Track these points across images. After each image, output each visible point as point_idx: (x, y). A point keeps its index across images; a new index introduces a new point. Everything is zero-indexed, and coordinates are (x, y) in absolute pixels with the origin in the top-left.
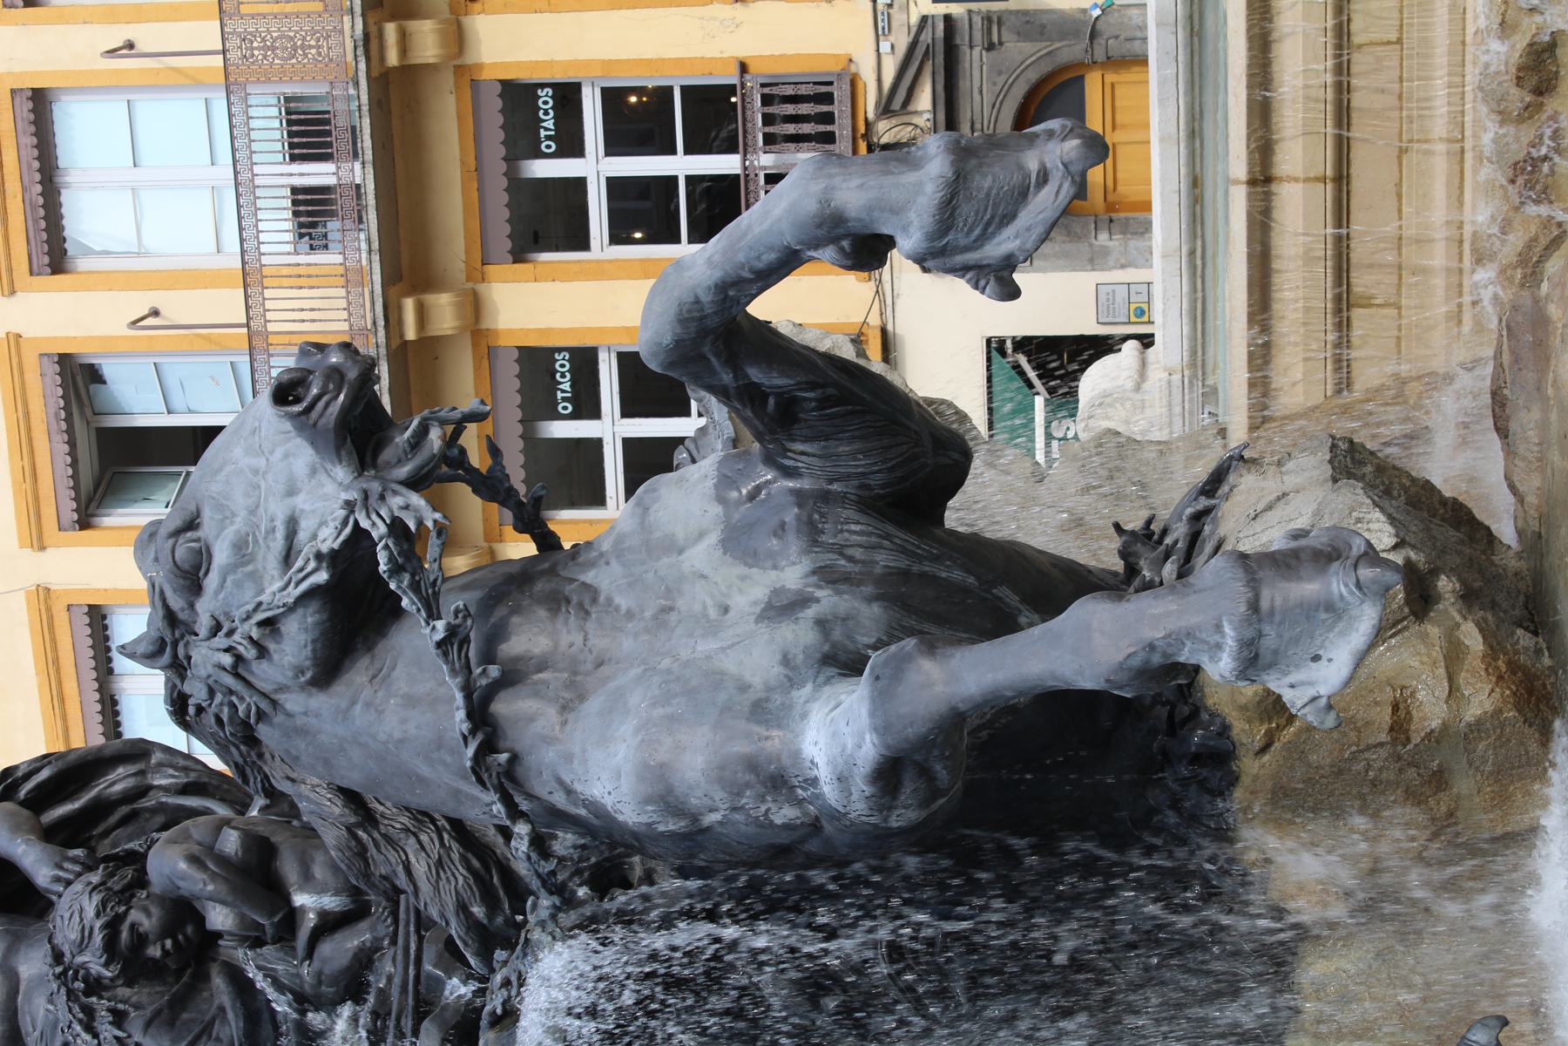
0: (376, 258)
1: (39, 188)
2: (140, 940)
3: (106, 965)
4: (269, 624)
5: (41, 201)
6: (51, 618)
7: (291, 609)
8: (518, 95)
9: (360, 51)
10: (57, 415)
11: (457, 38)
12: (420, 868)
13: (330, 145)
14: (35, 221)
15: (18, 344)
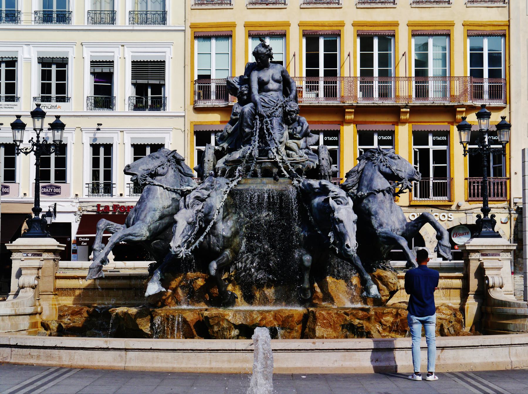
0: (309, 104)
2: (291, 115)
3: (288, 110)
4: (389, 167)
7: (391, 170)
8: (337, 133)
9: (350, 104)
10: (273, 32)
11: (349, 122)
12: (353, 179)
13: (331, 97)
14: (314, 32)
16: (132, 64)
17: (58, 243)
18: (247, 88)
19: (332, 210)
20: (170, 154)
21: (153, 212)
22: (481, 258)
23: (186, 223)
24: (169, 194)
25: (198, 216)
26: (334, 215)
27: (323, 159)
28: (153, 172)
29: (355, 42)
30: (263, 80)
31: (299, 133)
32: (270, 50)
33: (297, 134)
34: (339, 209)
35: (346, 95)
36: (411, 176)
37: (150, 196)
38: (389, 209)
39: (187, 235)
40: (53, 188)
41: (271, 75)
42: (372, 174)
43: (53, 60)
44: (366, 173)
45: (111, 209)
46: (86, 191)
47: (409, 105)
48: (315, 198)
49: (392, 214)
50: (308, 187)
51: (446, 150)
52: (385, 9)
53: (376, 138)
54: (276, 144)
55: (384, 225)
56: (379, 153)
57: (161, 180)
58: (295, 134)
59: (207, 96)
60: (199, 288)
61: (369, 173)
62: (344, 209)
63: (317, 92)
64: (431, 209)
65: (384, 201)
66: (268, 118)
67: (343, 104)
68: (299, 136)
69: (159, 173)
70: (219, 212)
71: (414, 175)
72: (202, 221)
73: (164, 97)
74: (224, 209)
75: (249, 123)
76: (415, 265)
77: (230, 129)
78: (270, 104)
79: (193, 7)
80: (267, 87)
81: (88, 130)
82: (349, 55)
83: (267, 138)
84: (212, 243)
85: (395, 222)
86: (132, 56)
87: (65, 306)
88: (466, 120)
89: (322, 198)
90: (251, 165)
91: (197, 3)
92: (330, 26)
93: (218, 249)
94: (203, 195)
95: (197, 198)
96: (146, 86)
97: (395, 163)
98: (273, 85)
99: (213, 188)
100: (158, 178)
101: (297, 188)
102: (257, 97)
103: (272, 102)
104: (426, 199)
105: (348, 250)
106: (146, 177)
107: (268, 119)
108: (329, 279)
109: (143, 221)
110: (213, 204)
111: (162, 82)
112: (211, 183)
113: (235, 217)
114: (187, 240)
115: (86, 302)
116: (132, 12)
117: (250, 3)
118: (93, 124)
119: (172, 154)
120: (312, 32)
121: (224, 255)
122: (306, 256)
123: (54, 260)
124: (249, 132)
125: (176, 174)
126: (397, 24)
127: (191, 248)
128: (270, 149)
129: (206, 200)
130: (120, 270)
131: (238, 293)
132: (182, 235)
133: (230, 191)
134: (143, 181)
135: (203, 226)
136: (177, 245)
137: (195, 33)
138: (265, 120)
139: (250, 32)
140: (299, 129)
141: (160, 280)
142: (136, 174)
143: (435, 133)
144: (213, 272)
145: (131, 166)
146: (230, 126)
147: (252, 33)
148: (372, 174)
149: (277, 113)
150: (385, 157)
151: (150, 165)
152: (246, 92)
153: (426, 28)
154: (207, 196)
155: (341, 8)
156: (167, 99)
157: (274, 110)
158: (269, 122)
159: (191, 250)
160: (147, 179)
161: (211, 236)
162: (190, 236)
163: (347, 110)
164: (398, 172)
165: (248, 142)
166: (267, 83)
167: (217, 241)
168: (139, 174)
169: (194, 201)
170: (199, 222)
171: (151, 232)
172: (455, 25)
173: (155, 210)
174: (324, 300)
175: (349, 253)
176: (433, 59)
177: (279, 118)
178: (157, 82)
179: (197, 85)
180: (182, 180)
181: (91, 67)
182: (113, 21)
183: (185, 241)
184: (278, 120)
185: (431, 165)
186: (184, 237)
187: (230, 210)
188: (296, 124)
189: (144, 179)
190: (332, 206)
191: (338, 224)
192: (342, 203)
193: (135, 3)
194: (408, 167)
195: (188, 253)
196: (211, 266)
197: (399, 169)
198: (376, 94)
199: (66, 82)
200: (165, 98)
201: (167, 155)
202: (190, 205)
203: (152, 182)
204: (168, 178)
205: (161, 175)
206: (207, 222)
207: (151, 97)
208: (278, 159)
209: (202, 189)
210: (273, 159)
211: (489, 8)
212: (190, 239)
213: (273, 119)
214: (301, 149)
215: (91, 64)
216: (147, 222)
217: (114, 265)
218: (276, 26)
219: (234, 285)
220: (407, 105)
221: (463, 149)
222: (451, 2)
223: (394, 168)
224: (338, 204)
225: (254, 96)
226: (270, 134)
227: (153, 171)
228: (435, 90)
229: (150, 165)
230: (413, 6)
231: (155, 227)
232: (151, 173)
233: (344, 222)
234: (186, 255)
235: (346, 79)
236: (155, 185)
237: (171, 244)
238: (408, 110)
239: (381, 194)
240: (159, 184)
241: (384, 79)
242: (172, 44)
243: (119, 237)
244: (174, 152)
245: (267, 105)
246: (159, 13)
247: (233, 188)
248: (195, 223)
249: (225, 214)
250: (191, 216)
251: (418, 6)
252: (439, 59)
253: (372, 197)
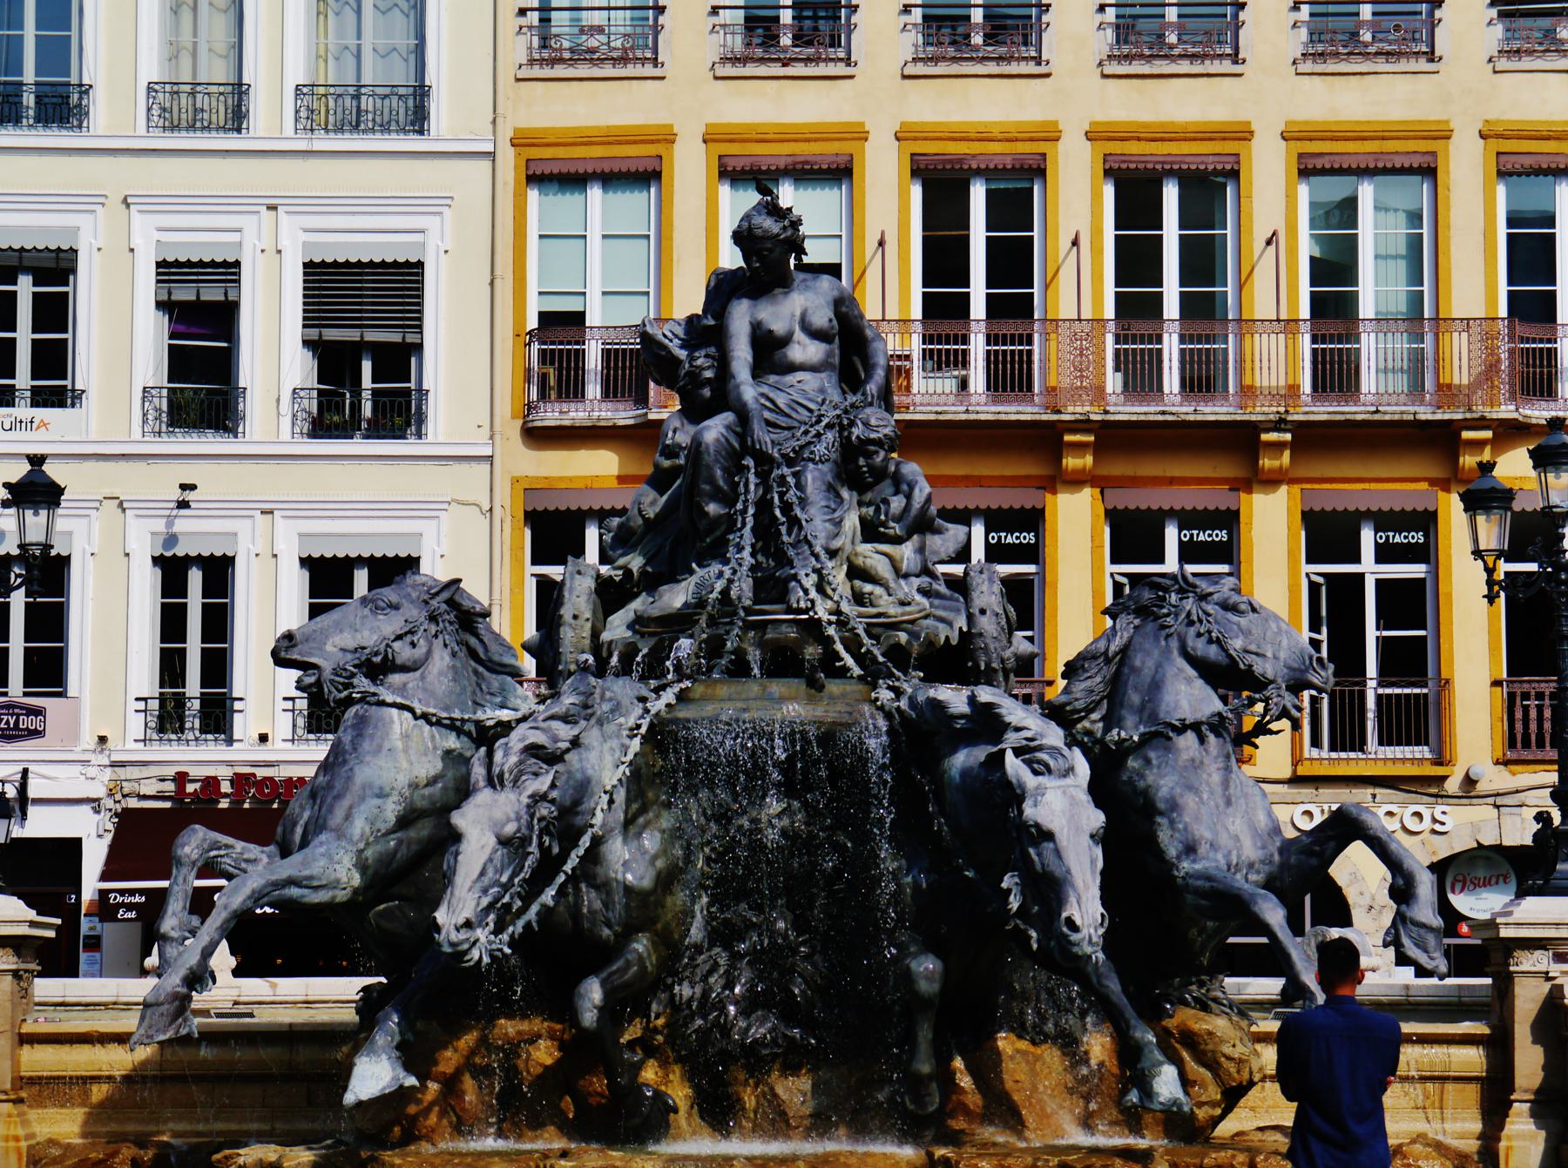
0: (932, 417)
1: (974, 166)
2: (869, 456)
3: (858, 437)
5: (966, 167)
6: (652, 142)
7: (1226, 651)
8: (1034, 519)
10: (807, 162)
11: (1076, 481)
12: (1088, 683)
13: (1013, 390)
14: (950, 161)
15: (861, 139)
16: (305, 274)
17: (31, 914)
18: (713, 358)
19: (1014, 795)
20: (437, 594)
21: (377, 801)
22: (1555, 969)
23: (492, 841)
24: (433, 737)
25: (538, 815)
26: (1021, 812)
27: (983, 612)
28: (377, 659)
29: (1097, 198)
30: (771, 332)
31: (898, 519)
32: (796, 224)
33: (892, 524)
34: (1040, 791)
35: (1066, 382)
36: (1298, 675)
37: (366, 745)
38: (1219, 790)
39: (497, 883)
40: (18, 715)
41: (798, 313)
42: (1159, 666)
43: (21, 258)
44: (1138, 663)
45: (226, 787)
46: (136, 725)
47: (1290, 418)
48: (954, 751)
49: (1230, 810)
50: (928, 714)
51: (1423, 580)
52: (1205, 79)
53: (1172, 535)
54: (817, 557)
55: (1203, 849)
56: (1181, 591)
57: (405, 685)
58: (884, 524)
59: (572, 389)
60: (539, 1077)
61: (1145, 662)
62: (1059, 792)
63: (964, 372)
64: (1370, 791)
65: (1202, 763)
66: (789, 466)
67: (1055, 417)
68: (896, 529)
69: (399, 661)
70: (611, 802)
71: (1306, 671)
72: (549, 834)
73: (420, 390)
74: (628, 792)
75: (721, 483)
76: (1312, 993)
77: (653, 503)
78: (794, 415)
79: (526, 72)
80: (785, 356)
81: (147, 507)
82: (1075, 243)
83: (785, 538)
84: (585, 911)
85: (1242, 838)
86: (305, 244)
87: (51, 1142)
88: (1495, 473)
89: (980, 753)
90: (728, 633)
91: (537, 56)
92: (1008, 140)
93: (606, 932)
94: (556, 740)
95: (533, 750)
96: (356, 350)
97: (1238, 625)
98: (805, 350)
99: (592, 715)
100: (396, 679)
101: (888, 716)
102: (749, 392)
103: (800, 410)
104: (1352, 755)
105: (1074, 937)
106: (353, 675)
107: (786, 470)
108: (1005, 1042)
109: (340, 834)
110: (590, 772)
111: (411, 338)
112: (582, 698)
113: (667, 821)
114: (496, 900)
115: (131, 1128)
116: (305, 90)
117: (725, 60)
118: (163, 483)
119: (445, 595)
120: (944, 162)
121: (630, 957)
122: (922, 958)
123: (16, 974)
124: (721, 516)
125: (459, 665)
126: (1244, 134)
127: (511, 929)
128: (796, 575)
129: (567, 757)
130: (256, 1010)
131: (680, 1093)
132: (479, 885)
133: (651, 726)
134: (340, 691)
135: (556, 850)
136: (461, 921)
137: (531, 163)
138: (776, 473)
139: (726, 160)
140: (897, 503)
141: (398, 1048)
143: (1384, 521)
144: (589, 1018)
145: (298, 637)
146: (652, 494)
147: (731, 164)
148: (1159, 666)
149: (820, 449)
150: (1203, 604)
151: (366, 633)
152: (708, 374)
153: (1351, 147)
154: (567, 745)
155: (1048, 75)
156: (431, 396)
157: (808, 438)
158: (791, 480)
159: (512, 936)
160: (355, 681)
161: (583, 886)
162: (506, 887)
163: (1068, 438)
164: (1251, 659)
165: (718, 552)
166: (786, 341)
167: (606, 905)
168: (327, 666)
169: (521, 762)
170: (540, 837)
171: (370, 872)
172: (1455, 136)
173: (382, 795)
174: (987, 1117)
175: (1075, 949)
176: (1377, 257)
177: (825, 468)
178: (394, 337)
179: (536, 347)
180: (479, 685)
181: (158, 281)
182: (237, 119)
183: (490, 907)
184: (823, 474)
185: (1372, 633)
187: (650, 795)
188: (886, 488)
189: (343, 684)
190: (1014, 781)
191: (1036, 845)
192: (1049, 771)
193: (318, 57)
194: (1285, 643)
195: (500, 950)
196: (581, 996)
197: (1253, 648)
198: (1171, 380)
199: (69, 336)
200: (422, 393)
201: (426, 597)
202: (506, 775)
203: (374, 694)
204: (430, 678)
205: (405, 669)
206: (570, 837)
207: (373, 390)
208: (822, 611)
209: (552, 717)
210: (806, 611)
212: (506, 899)
213: (805, 467)
214: (906, 576)
215: (158, 274)
216: (356, 838)
217: (235, 992)
218: (816, 140)
219: (664, 1064)
220: (1282, 421)
221: (1485, 576)
222: (1437, 54)
223: (1236, 644)
224: (1036, 773)
225: (737, 386)
226: (794, 522)
227: (376, 654)
228: (1381, 365)
229: (366, 633)
230: (1302, 68)
231: (381, 854)
232: (368, 660)
233: (1058, 836)
234: (491, 956)
235: (1063, 329)
236: (383, 703)
237: (441, 916)
238: (1288, 437)
239: (1190, 736)
240: (399, 700)
241: (1201, 328)
242: (448, 202)
243: (253, 892)
244: (453, 588)
245: (783, 421)
246: (402, 91)
247: (663, 714)
248: (525, 841)
249: (635, 806)
250: (513, 816)
251: (1320, 68)
252: (1395, 257)
253: (1156, 749)
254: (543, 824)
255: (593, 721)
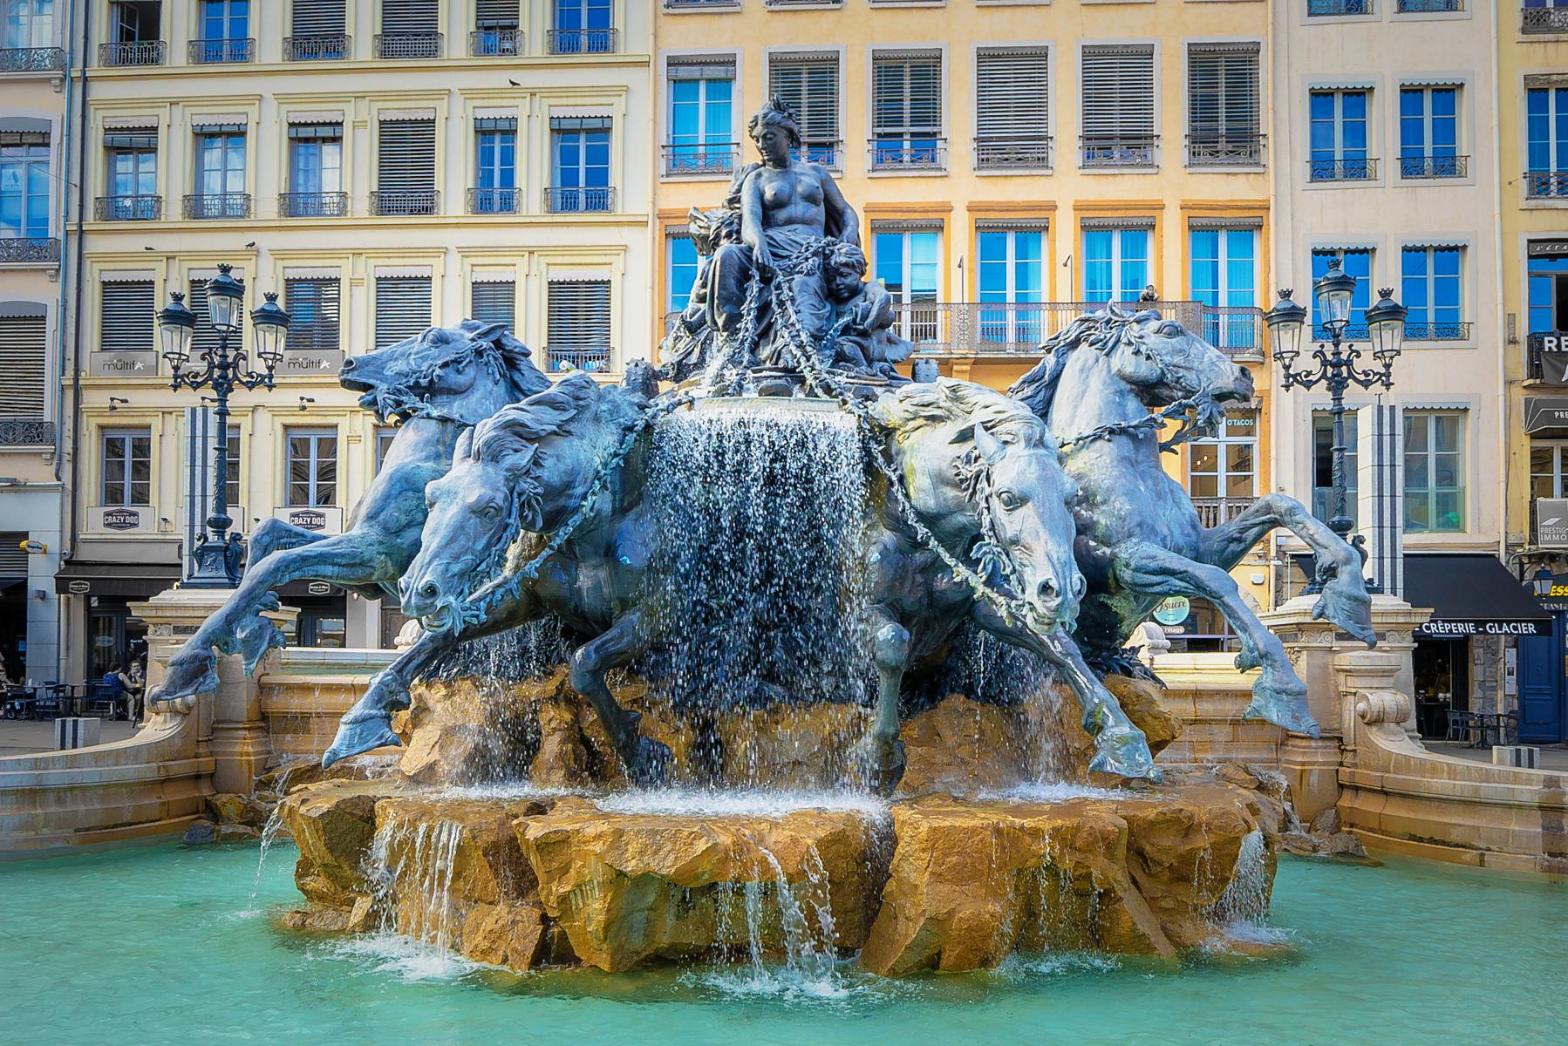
25: (517, 488)
67: (949, 356)
92: (924, 212)
119: (494, 337)
142: (371, 387)
153: (1109, 214)
186: (456, 558)
211: (1230, 176)
232: (417, 383)
254: (523, 498)
255: (587, 415)
